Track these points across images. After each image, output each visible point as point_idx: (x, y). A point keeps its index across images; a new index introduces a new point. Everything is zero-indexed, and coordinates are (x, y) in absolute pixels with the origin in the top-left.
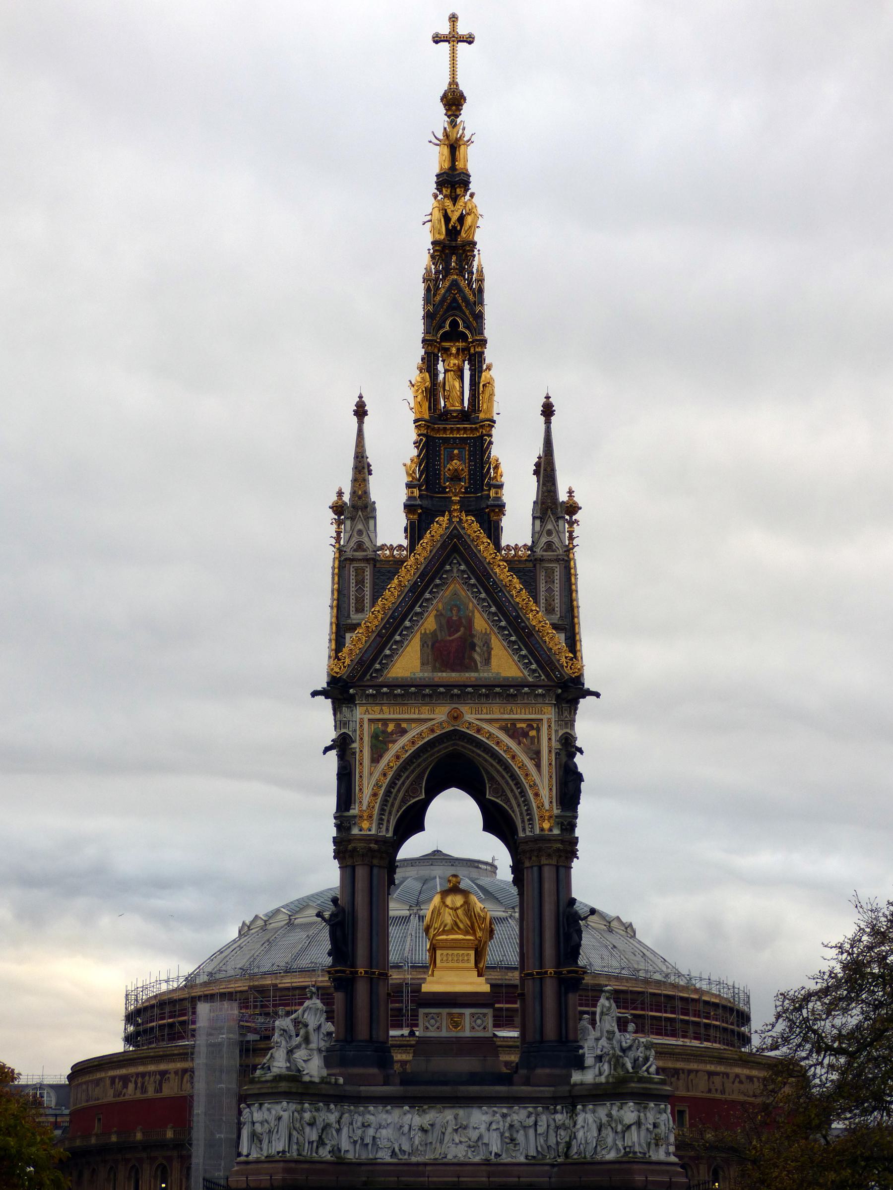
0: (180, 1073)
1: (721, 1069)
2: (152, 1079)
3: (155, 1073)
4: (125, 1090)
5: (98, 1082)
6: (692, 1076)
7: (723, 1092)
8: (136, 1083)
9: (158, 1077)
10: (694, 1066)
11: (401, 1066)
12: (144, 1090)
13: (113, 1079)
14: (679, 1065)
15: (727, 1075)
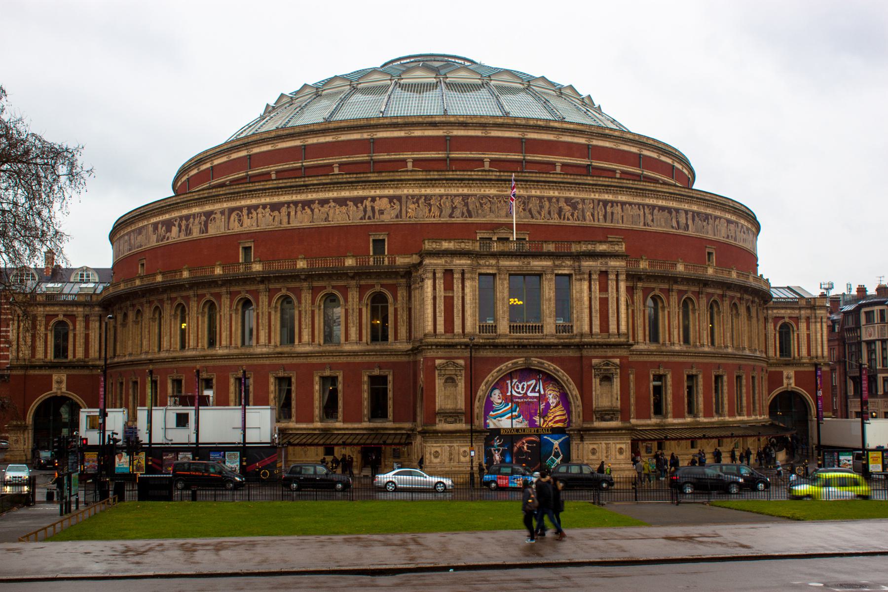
0: (226, 213)
1: (734, 218)
2: (197, 221)
3: (199, 214)
4: (168, 234)
5: (140, 231)
6: (718, 221)
7: (735, 240)
8: (180, 226)
9: (203, 218)
10: (718, 213)
11: (463, 200)
12: (188, 231)
13: (155, 226)
14: (709, 211)
15: (737, 223)
